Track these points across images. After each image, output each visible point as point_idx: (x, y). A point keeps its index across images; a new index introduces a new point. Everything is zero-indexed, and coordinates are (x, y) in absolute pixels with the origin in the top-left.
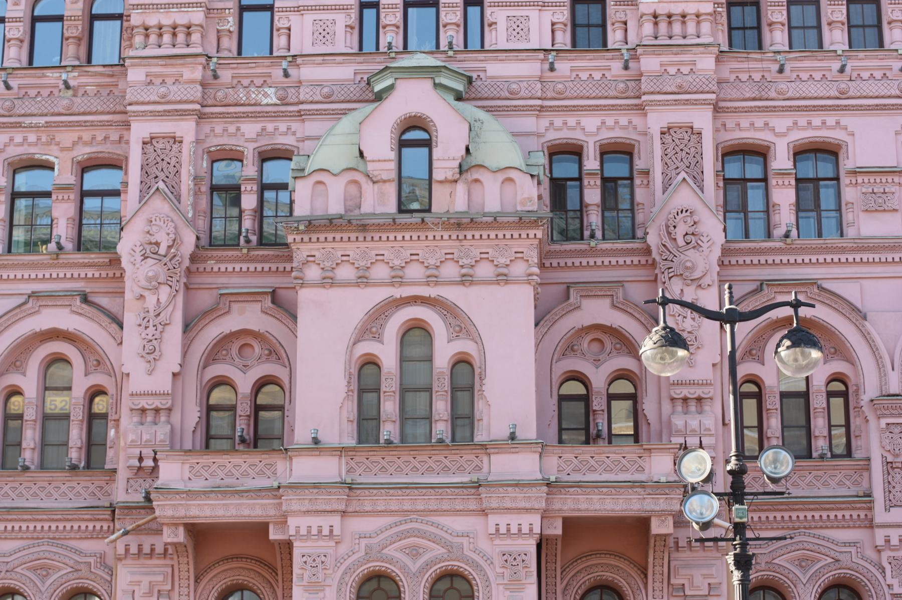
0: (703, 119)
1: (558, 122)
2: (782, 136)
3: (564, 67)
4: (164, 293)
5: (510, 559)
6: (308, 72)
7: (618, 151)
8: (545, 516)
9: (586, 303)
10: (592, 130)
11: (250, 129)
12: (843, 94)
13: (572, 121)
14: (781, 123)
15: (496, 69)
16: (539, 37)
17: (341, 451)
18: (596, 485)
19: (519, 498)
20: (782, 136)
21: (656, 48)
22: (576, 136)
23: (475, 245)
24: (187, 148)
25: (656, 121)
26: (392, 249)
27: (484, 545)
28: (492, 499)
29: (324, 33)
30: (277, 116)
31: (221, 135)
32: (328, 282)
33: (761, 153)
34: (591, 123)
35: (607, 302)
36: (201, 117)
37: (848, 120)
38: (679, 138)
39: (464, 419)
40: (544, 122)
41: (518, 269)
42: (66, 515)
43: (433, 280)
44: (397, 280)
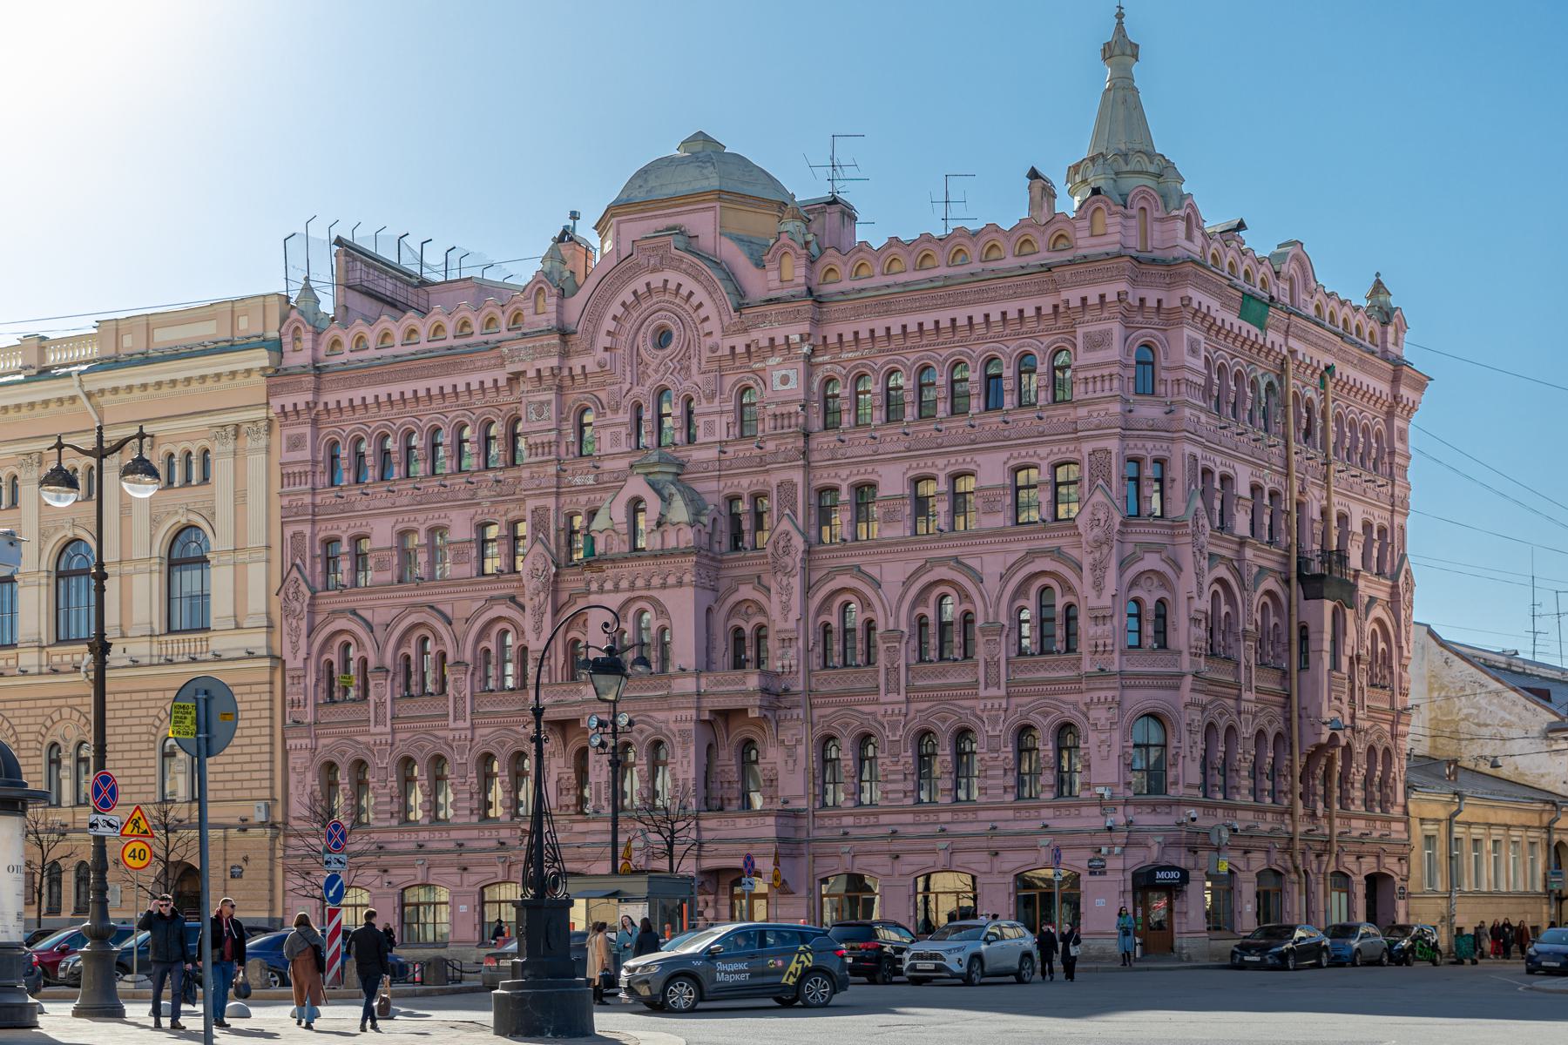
0: (797, 477)
2: (844, 479)
3: (730, 450)
5: (682, 733)
6: (608, 465)
7: (756, 497)
8: (698, 709)
9: (742, 588)
10: (745, 485)
11: (583, 498)
12: (876, 453)
14: (844, 473)
16: (720, 434)
18: (722, 694)
19: (684, 702)
20: (844, 479)
21: (773, 437)
23: (668, 565)
24: (552, 513)
25: (774, 480)
26: (627, 570)
27: (672, 726)
28: (674, 702)
29: (615, 440)
30: (593, 491)
31: (568, 503)
33: (834, 489)
34: (745, 482)
36: (558, 494)
37: (879, 468)
38: (786, 488)
40: (722, 484)
41: (687, 578)
42: (510, 714)
44: (632, 587)
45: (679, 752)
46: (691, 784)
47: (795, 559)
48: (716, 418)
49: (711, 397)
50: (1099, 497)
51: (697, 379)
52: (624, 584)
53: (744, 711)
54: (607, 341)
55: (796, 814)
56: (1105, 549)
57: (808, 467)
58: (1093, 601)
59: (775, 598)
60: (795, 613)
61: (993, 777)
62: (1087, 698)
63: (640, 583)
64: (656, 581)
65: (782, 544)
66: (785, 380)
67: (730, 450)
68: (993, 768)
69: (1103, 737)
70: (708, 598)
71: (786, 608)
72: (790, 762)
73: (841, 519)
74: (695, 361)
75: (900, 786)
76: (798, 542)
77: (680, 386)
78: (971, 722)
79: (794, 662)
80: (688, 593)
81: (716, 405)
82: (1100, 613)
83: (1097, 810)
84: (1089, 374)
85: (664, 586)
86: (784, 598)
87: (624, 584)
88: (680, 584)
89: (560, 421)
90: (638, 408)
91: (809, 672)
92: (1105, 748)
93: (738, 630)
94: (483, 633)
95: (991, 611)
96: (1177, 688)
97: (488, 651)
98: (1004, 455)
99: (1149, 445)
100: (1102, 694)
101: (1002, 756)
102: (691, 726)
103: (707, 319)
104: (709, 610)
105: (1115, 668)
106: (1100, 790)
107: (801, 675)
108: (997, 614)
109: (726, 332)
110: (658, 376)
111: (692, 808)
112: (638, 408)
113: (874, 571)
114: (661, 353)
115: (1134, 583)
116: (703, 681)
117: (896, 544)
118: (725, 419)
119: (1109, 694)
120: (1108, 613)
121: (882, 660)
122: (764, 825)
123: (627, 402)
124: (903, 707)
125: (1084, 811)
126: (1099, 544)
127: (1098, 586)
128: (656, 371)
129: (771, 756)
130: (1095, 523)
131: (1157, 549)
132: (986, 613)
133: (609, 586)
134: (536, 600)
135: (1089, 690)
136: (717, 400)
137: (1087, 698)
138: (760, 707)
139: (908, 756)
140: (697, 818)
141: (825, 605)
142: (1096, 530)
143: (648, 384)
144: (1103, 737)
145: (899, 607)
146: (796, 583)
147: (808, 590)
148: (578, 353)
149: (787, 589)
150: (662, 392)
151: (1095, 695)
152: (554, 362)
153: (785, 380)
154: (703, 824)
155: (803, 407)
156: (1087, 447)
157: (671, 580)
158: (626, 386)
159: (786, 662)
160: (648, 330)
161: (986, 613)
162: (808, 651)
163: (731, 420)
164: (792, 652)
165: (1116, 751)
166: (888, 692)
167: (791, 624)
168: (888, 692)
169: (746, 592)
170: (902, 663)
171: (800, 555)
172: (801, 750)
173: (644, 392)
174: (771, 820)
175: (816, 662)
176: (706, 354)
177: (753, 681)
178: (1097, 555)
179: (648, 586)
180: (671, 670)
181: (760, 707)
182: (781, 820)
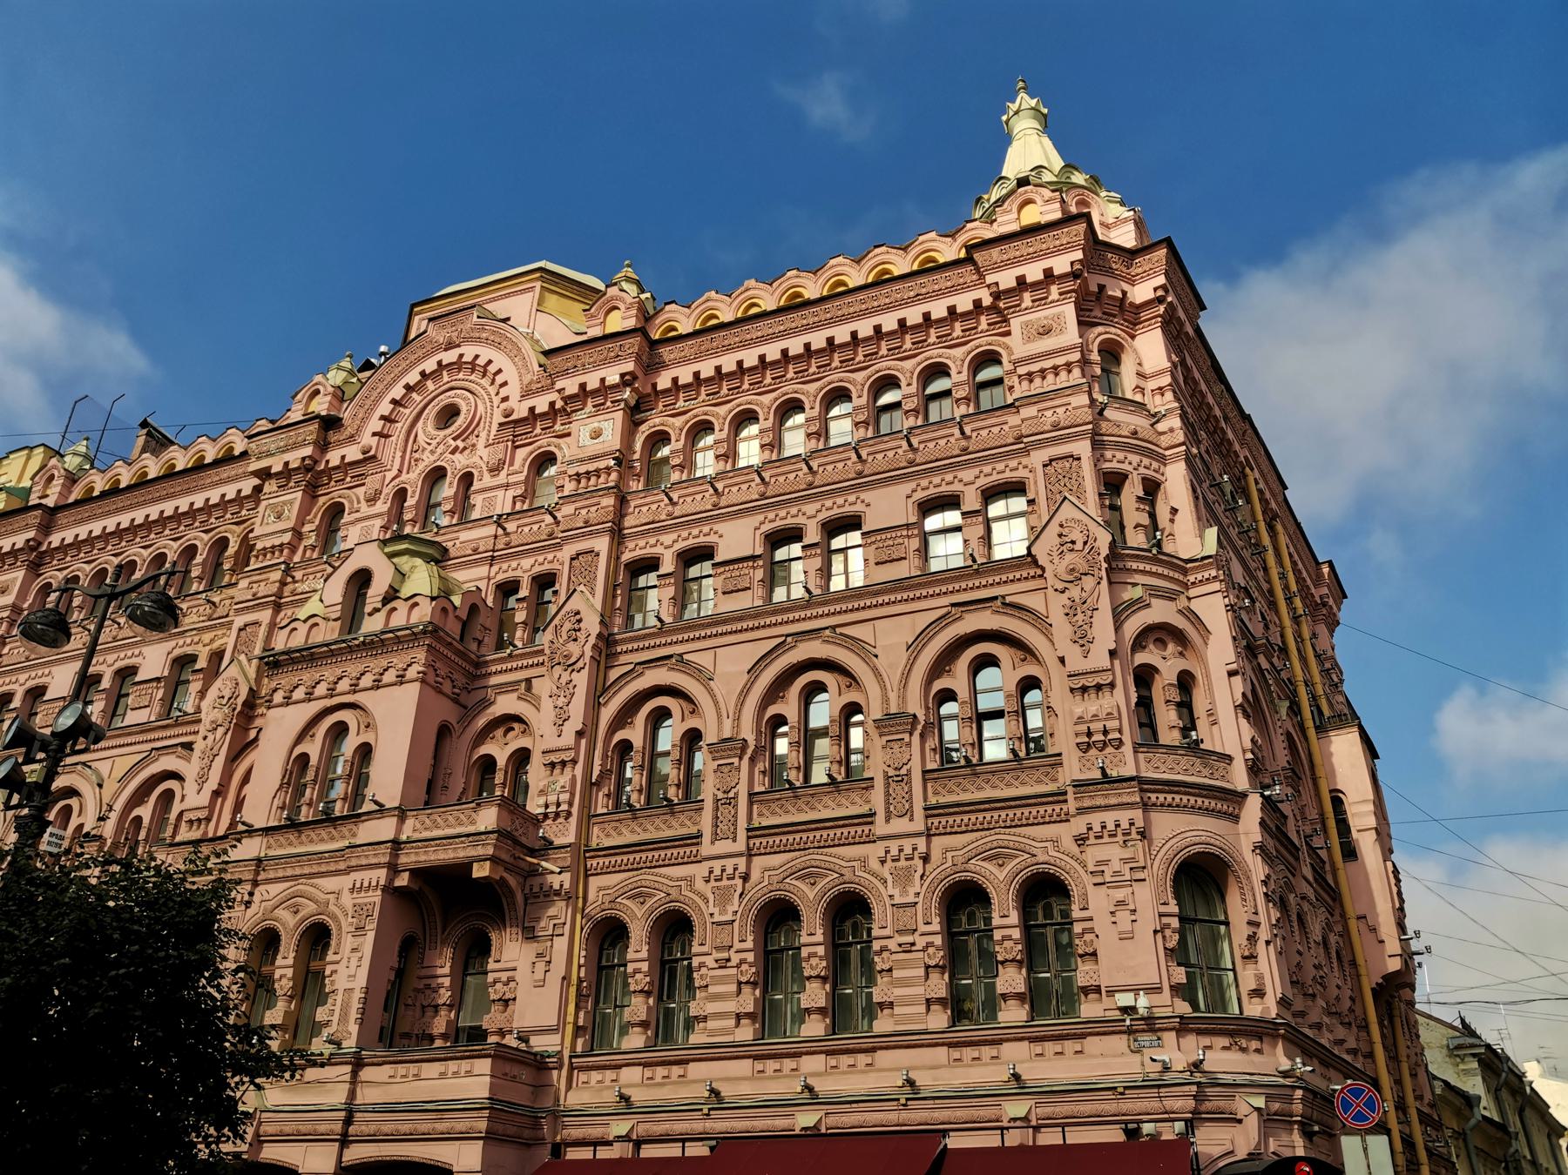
0: (602, 544)
1: (505, 566)
3: (511, 526)
4: (221, 731)
7: (545, 581)
8: (393, 869)
9: (500, 698)
10: (525, 569)
13: (514, 564)
15: (465, 535)
17: (267, 831)
22: (518, 573)
32: (288, 701)
34: (526, 563)
35: (515, 695)
36: (278, 607)
39: (357, 796)
40: (495, 568)
43: (355, 688)
44: (332, 692)
45: (348, 942)
46: (358, 995)
47: (584, 649)
48: (500, 493)
49: (495, 470)
50: (1067, 512)
51: (480, 456)
52: (321, 690)
53: (467, 866)
54: (375, 424)
55: (540, 1064)
56: (1088, 582)
57: (618, 535)
58: (1076, 662)
59: (547, 704)
60: (575, 724)
61: (905, 983)
62: (1079, 825)
63: (344, 685)
64: (367, 681)
65: (568, 626)
66: (596, 434)
67: (511, 526)
68: (904, 965)
69: (1120, 894)
70: (446, 711)
71: (562, 720)
72: (541, 966)
73: (657, 600)
74: (483, 435)
75: (731, 1006)
76: (592, 625)
77: (458, 463)
78: (865, 882)
79: (565, 797)
80: (412, 692)
81: (502, 478)
82: (1090, 681)
83: (1119, 1043)
84: (1035, 367)
85: (377, 685)
86: (561, 701)
87: (321, 690)
88: (401, 680)
89: (301, 520)
90: (401, 494)
91: (588, 818)
92: (1124, 917)
93: (489, 763)
94: (139, 797)
95: (893, 696)
96: (1235, 818)
97: (139, 819)
98: (907, 487)
99: (1135, 459)
100: (1109, 818)
101: (921, 942)
102: (376, 897)
103: (505, 384)
104: (444, 731)
105: (1129, 771)
106: (1125, 999)
107: (573, 820)
108: (903, 698)
109: (527, 394)
110: (433, 458)
111: (350, 1044)
112: (401, 494)
113: (704, 659)
114: (442, 433)
115: (1139, 643)
116: (410, 823)
117: (740, 619)
118: (511, 493)
119: (1124, 816)
120: (1105, 679)
121: (708, 790)
122: (469, 1074)
123: (388, 491)
124: (742, 862)
125: (1092, 1044)
126: (1076, 576)
127: (1083, 640)
128: (432, 452)
129: (510, 951)
130: (1067, 545)
131: (1170, 596)
132: (886, 700)
133: (299, 694)
134: (211, 737)
135: (1082, 811)
136: (504, 473)
137: (1079, 825)
138: (493, 859)
139: (745, 945)
140: (358, 1064)
141: (624, 716)
142: (1069, 557)
143: (421, 466)
144: (1120, 894)
145: (741, 703)
146: (581, 680)
147: (599, 693)
148: (340, 444)
149: (568, 689)
150: (437, 475)
151: (1095, 819)
152: (308, 451)
153: (596, 434)
154: (367, 1074)
155: (619, 462)
156: (1039, 457)
157: (390, 677)
158: (389, 475)
159: (552, 798)
160: (432, 412)
161: (886, 700)
162: (591, 786)
163: (519, 492)
164: (563, 779)
165: (1147, 922)
166: (715, 838)
167: (568, 738)
168: (715, 838)
169: (506, 704)
170: (743, 790)
171: (592, 640)
172: (561, 944)
173: (413, 480)
174: (484, 1065)
175: (601, 805)
176: (498, 418)
177: (488, 818)
178: (1075, 592)
179: (355, 688)
180: (368, 806)
181: (493, 859)
182: (508, 1068)
